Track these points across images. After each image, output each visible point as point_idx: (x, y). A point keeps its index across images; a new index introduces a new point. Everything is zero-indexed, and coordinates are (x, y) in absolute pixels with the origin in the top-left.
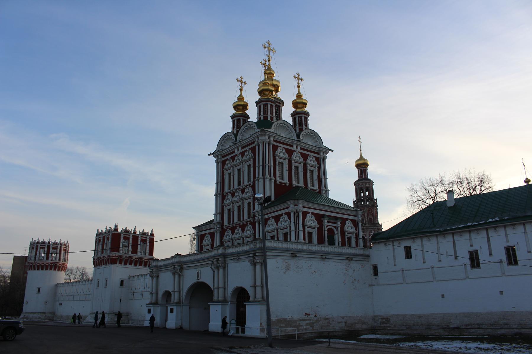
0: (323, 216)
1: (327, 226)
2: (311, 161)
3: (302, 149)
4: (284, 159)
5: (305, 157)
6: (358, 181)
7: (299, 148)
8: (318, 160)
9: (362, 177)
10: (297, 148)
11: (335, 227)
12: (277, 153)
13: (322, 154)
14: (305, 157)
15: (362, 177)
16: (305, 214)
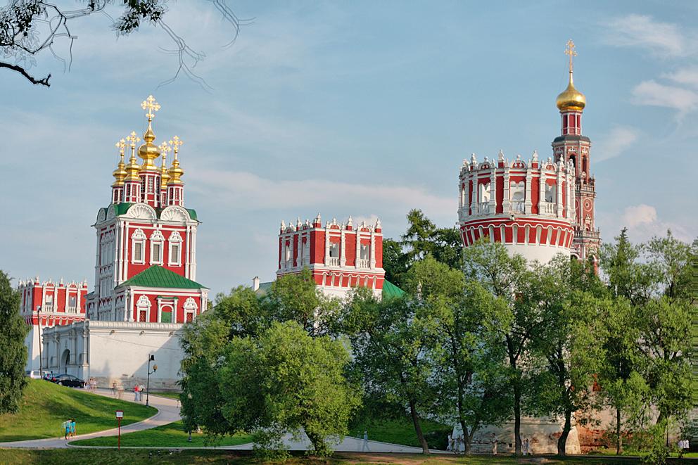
0: (157, 296)
1: (162, 305)
2: (175, 238)
3: (163, 226)
4: (142, 240)
5: (167, 234)
6: (557, 140)
7: (160, 226)
8: (183, 235)
9: (565, 131)
10: (158, 226)
11: (173, 305)
12: (134, 236)
13: (188, 227)
14: (167, 234)
15: (565, 131)
16: (137, 297)
